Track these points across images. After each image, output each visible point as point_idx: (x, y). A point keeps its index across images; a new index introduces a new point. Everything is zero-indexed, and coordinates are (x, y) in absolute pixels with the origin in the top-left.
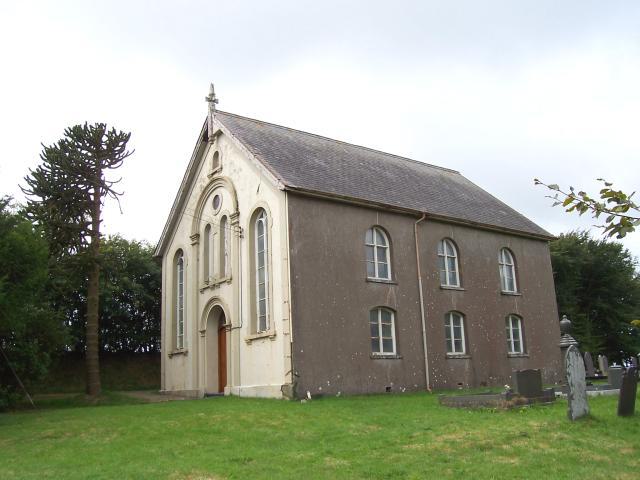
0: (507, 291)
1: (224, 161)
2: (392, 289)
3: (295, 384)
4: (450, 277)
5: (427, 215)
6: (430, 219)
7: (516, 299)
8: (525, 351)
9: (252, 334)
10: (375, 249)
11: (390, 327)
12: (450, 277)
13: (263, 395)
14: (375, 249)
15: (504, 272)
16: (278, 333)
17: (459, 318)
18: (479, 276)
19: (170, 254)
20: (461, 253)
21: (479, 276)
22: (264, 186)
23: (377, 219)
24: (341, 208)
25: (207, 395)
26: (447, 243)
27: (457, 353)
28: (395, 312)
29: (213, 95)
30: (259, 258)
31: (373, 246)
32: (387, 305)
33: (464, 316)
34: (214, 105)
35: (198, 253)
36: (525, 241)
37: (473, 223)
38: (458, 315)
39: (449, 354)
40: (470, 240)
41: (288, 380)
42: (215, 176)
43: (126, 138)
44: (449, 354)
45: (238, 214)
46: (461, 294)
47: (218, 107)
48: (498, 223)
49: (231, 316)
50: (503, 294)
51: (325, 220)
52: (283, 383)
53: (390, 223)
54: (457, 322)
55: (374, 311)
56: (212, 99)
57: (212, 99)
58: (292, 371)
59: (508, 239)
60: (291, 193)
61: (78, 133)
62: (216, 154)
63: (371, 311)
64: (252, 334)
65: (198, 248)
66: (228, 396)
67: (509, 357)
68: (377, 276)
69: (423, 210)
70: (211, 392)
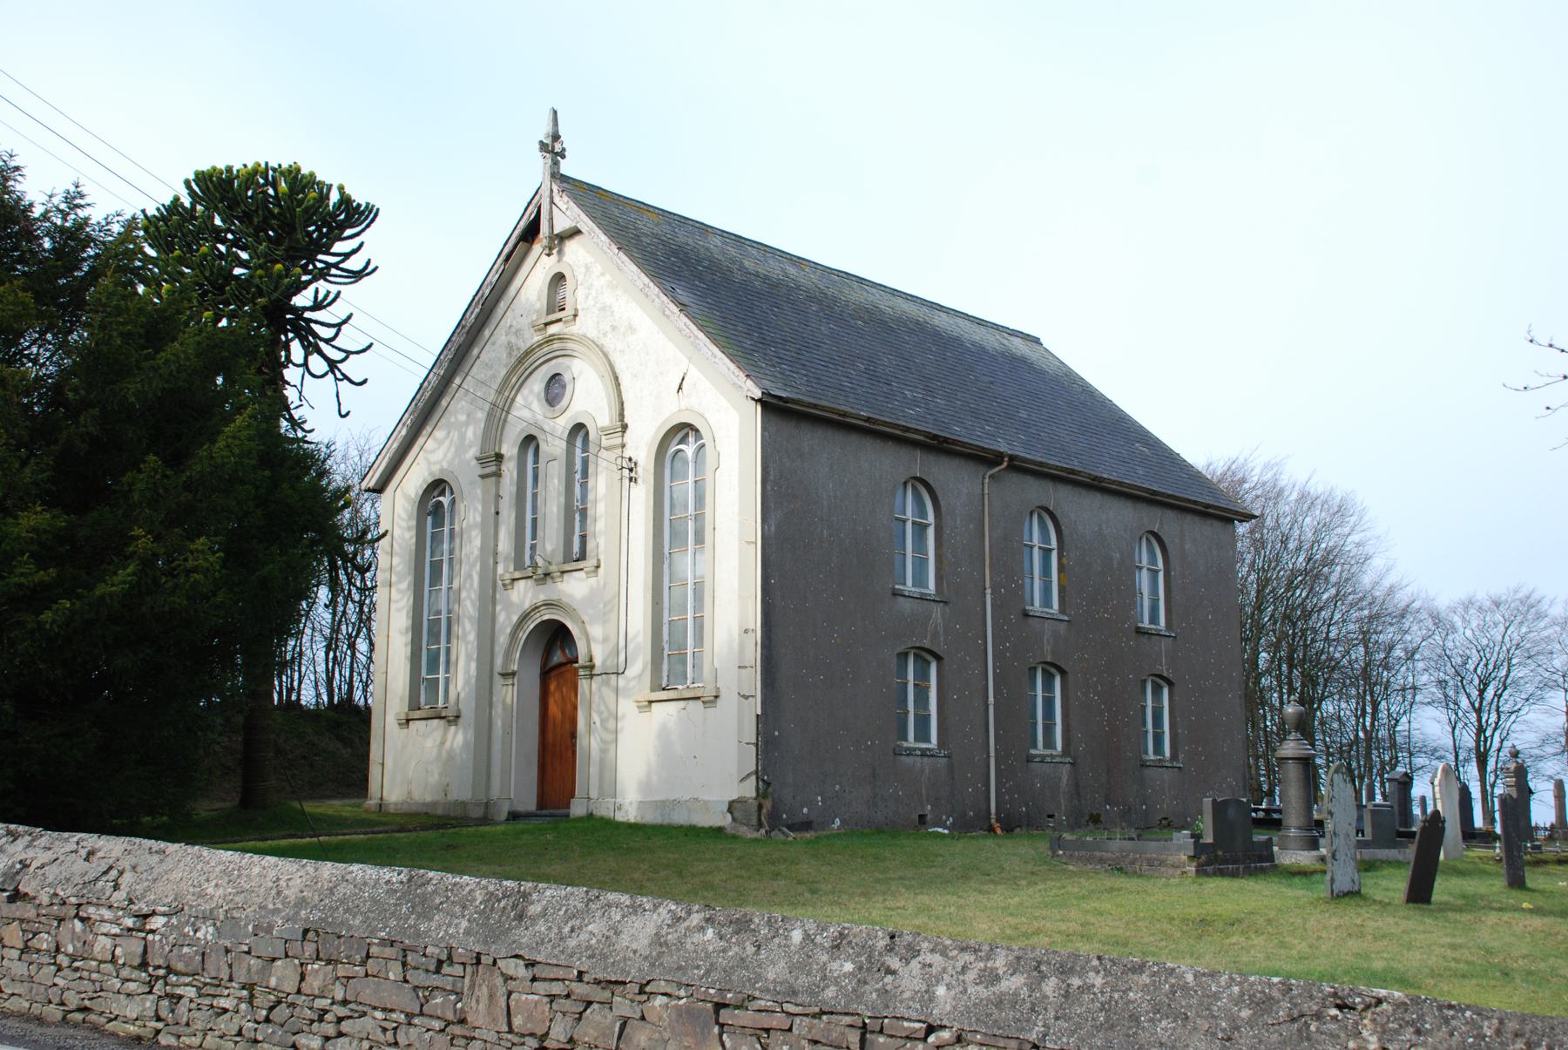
0: (1146, 624)
1: (577, 295)
2: (937, 611)
3: (761, 795)
4: (1043, 593)
5: (1012, 458)
6: (1018, 466)
7: (1164, 643)
8: (1174, 756)
9: (653, 690)
10: (909, 526)
11: (928, 688)
12: (1043, 593)
13: (680, 818)
14: (909, 526)
15: (1144, 579)
16: (723, 693)
17: (1053, 676)
18: (1096, 587)
19: (555, 525)
20: (1067, 540)
21: (1096, 587)
22: (694, 375)
23: (917, 463)
24: (854, 440)
25: (514, 816)
26: (1040, 516)
27: (1048, 752)
28: (939, 658)
29: (556, 137)
30: (675, 530)
31: (904, 521)
32: (927, 644)
33: (1063, 672)
34: (556, 163)
35: (498, 497)
36: (1189, 517)
37: (1096, 478)
38: (1053, 669)
39: (1033, 752)
40: (1083, 511)
41: (749, 790)
42: (553, 329)
43: (355, 215)
44: (1033, 752)
45: (625, 427)
46: (1063, 626)
47: (566, 168)
48: (1139, 478)
49: (593, 642)
50: (1140, 632)
51: (826, 456)
52: (735, 797)
53: (943, 472)
54: (1048, 686)
55: (903, 656)
56: (552, 148)
57: (552, 148)
58: (757, 772)
59: (1158, 512)
60: (771, 407)
61: (216, 188)
62: (559, 278)
63: (899, 655)
64: (653, 690)
65: (498, 485)
66: (580, 819)
67: (1144, 765)
68: (909, 582)
69: (1003, 447)
70: (521, 808)
